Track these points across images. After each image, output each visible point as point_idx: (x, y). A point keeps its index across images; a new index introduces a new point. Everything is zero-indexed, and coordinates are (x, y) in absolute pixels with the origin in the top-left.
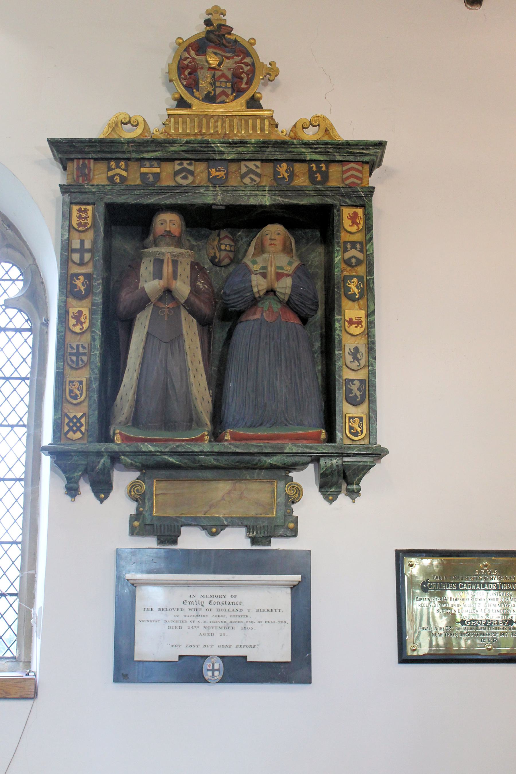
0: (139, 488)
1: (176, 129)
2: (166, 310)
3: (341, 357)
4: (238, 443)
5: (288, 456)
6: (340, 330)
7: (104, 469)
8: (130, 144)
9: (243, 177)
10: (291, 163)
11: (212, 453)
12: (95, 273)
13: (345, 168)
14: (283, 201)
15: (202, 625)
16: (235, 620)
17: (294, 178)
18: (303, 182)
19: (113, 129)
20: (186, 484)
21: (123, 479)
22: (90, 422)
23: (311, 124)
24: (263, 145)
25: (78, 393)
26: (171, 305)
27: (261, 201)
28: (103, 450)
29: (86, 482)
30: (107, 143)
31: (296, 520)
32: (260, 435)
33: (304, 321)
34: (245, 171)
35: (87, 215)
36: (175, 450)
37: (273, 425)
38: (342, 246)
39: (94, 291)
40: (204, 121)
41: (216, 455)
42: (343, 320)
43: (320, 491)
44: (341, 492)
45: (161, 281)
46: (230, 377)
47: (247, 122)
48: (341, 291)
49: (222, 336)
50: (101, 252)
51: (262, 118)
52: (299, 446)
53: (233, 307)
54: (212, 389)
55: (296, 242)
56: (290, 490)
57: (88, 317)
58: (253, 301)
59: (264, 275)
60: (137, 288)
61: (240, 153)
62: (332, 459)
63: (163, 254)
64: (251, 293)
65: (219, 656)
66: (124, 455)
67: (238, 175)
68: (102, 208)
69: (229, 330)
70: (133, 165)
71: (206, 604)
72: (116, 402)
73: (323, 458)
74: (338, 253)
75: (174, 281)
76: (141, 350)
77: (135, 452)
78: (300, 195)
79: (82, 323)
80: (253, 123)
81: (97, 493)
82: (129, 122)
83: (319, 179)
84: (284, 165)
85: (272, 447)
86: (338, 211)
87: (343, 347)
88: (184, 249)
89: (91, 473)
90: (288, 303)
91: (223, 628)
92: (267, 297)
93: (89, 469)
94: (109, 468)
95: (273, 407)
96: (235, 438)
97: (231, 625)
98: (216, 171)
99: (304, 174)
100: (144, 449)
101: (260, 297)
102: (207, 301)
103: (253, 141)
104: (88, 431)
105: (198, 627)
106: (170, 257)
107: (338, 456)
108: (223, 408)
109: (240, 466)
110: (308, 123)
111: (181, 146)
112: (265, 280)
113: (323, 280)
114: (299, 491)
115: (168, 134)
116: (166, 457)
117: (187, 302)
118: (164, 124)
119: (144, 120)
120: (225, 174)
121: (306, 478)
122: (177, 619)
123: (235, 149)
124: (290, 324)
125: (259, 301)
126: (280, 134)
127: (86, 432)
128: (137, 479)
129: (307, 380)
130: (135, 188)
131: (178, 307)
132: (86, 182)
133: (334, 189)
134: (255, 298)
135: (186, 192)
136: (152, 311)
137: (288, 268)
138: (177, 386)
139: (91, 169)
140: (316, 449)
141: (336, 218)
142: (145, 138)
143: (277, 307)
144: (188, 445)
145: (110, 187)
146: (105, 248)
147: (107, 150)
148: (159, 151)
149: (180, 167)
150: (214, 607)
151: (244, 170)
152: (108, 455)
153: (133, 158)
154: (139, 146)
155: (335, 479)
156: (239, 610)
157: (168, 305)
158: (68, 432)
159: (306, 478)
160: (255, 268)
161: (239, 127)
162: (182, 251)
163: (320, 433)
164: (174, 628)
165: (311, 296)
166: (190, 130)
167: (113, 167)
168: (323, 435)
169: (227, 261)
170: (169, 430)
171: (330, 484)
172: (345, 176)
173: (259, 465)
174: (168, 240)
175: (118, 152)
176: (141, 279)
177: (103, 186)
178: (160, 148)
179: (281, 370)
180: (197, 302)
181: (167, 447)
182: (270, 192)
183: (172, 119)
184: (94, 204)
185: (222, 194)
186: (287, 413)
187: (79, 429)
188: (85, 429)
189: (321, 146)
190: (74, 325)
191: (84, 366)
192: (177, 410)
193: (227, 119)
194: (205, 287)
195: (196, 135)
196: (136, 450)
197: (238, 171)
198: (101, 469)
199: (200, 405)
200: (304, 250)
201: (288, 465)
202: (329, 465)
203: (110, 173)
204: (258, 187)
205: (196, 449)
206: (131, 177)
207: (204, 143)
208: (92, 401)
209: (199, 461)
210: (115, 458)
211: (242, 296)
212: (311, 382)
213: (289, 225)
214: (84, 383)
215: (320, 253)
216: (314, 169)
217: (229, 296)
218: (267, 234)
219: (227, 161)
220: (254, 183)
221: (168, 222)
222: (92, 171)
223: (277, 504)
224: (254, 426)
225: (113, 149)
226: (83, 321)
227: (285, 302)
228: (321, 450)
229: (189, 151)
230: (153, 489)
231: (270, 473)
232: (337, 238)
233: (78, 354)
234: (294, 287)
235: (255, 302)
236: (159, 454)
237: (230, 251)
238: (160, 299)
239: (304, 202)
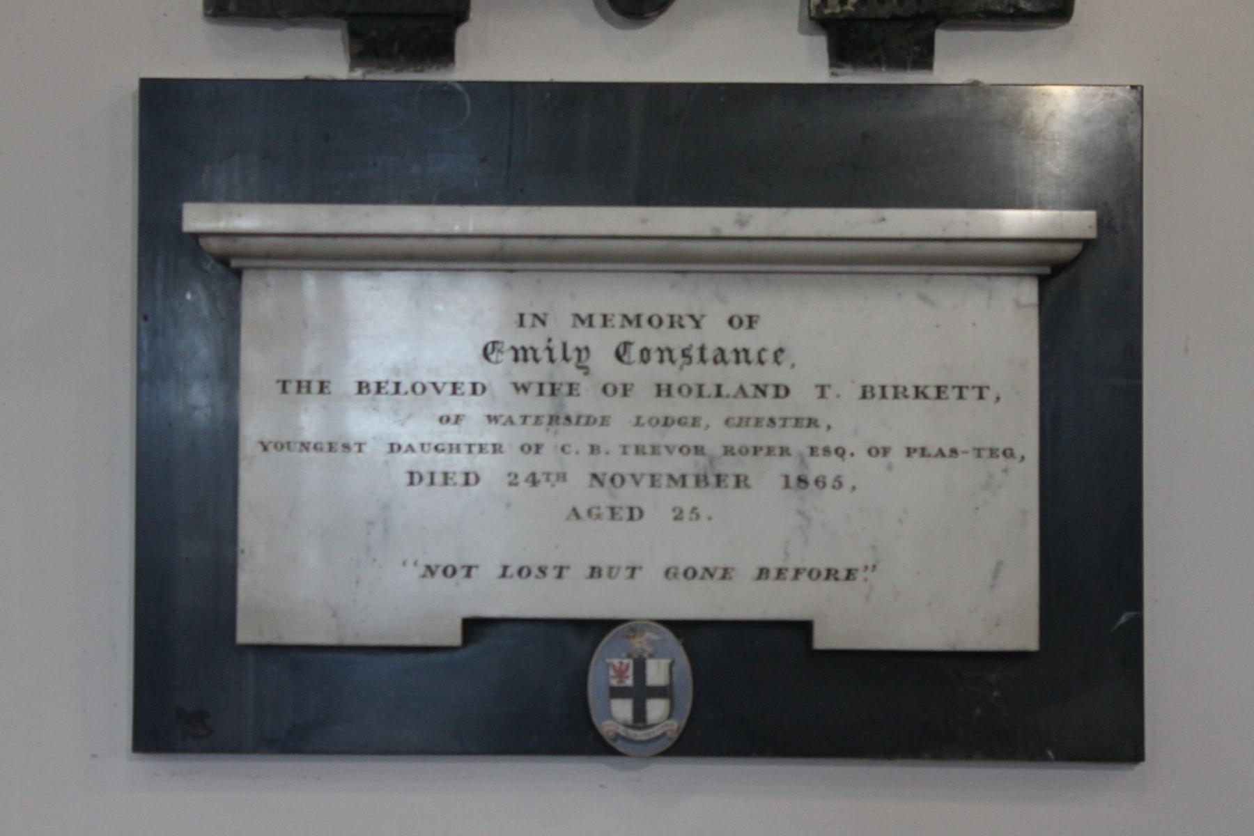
15: (579, 467)
16: (750, 443)
65: (672, 625)
71: (604, 366)
91: (691, 481)
97: (729, 466)
105: (562, 477)
122: (451, 434)
150: (644, 375)
156: (771, 391)
164: (439, 479)
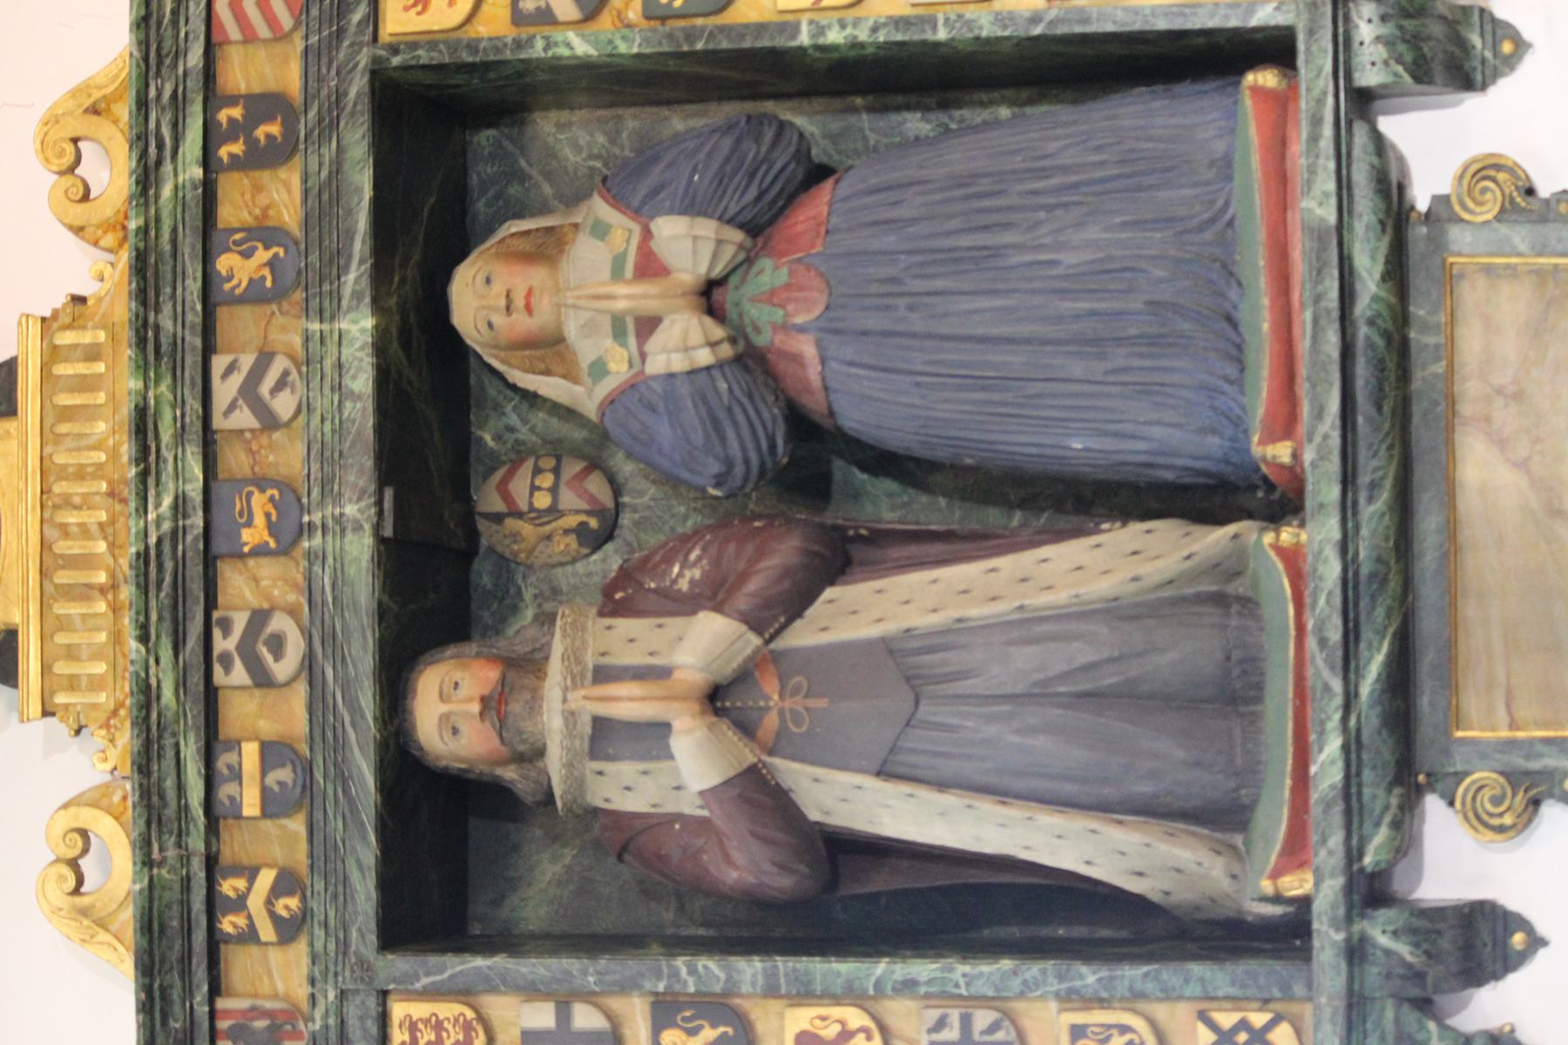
0: (1486, 794)
1: (96, 684)
2: (787, 704)
3: (960, 16)
4: (1305, 410)
5: (1350, 212)
6: (855, 25)
7: (1414, 931)
8: (156, 855)
9: (269, 421)
10: (216, 239)
11: (1348, 509)
12: (648, 985)
13: (234, 33)
14: (361, 262)
17: (271, 223)
18: (289, 192)
19: (102, 924)
20: (1469, 610)
21: (1454, 860)
22: (1232, 991)
23: (71, 170)
24: (147, 341)
26: (770, 686)
27: (362, 348)
28: (1340, 937)
29: (1464, 1005)
30: (151, 942)
32: (1274, 324)
33: (819, 173)
34: (245, 408)
35: (426, 1022)
36: (1339, 654)
37: (1232, 274)
38: (532, 30)
39: (717, 988)
40: (63, 577)
41: (1355, 493)
42: (816, 16)
43: (1484, 87)
44: (1482, 11)
45: (677, 725)
46: (1048, 452)
47: (66, 414)
48: (703, 29)
49: (890, 495)
50: (570, 964)
51: (53, 354)
52: (1312, 170)
53: (772, 447)
54: (1098, 524)
55: (519, 215)
56: (1481, 204)
57: (823, 1011)
58: (747, 369)
59: (648, 325)
60: (704, 823)
61: (181, 435)
62: (1356, 39)
63: (570, 717)
64: (716, 373)
66: (1361, 855)
67: (264, 440)
68: (399, 963)
69: (864, 469)
70: (234, 845)
72: (1155, 897)
73: (1356, 75)
74: (556, 44)
75: (677, 675)
76: (949, 800)
77: (1348, 812)
78: (337, 198)
80: (72, 390)
81: (1508, 962)
82: (73, 864)
83: (274, 129)
84: (224, 263)
85: (1319, 272)
86: (394, 49)
87: (921, 11)
88: (549, 644)
89: (1430, 980)
90: (754, 229)
92: (732, 313)
93: (1415, 992)
94: (1412, 914)
95: (1159, 273)
96: (1285, 423)
98: (249, 524)
99: (258, 189)
100: (1336, 775)
101: (733, 340)
102: (750, 548)
103: (135, 384)
104: (1266, 1001)
106: (583, 692)
107: (1347, 18)
108: (1169, 476)
109: (1395, 396)
110: (68, 180)
111: (157, 662)
112: (666, 323)
113: (665, 112)
114: (1486, 170)
115: (115, 713)
116: (1367, 687)
117: (755, 623)
118: (78, 732)
119: (65, 806)
120: (262, 491)
121: (1433, 143)
123: (164, 452)
124: (834, 220)
125: (749, 343)
126: (107, 285)
127: (1272, 1006)
128: (1451, 804)
129: (1052, 147)
130: (318, 838)
131: (776, 657)
132: (301, 1025)
133: (313, 70)
134: (738, 359)
135: (329, 638)
136: (794, 758)
137: (618, 238)
138: (1083, 654)
139: (253, 1009)
140: (1320, 101)
141: (424, 56)
142: (130, 803)
143: (770, 274)
144: (1315, 603)
145: (319, 933)
146: (555, 952)
147: (177, 947)
148: (177, 745)
149: (238, 665)
151: (244, 418)
152: (1363, 916)
153: (208, 844)
154: (160, 820)
155: (1436, 29)
157: (767, 698)
159: (1433, 143)
160: (619, 368)
161: (82, 443)
162: (558, 648)
163: (1257, 91)
165: (727, 143)
166: (98, 629)
167: (241, 921)
168: (1266, 78)
169: (597, 485)
170: (1260, 687)
171: (1454, 49)
172: (263, 31)
173: (1389, 325)
174: (516, 707)
175: (186, 905)
176: (669, 808)
177: (314, 959)
178: (168, 741)
179: (1017, 247)
180: (753, 585)
181: (1327, 688)
182: (327, 314)
183: (61, 699)
184: (384, 994)
185: (338, 499)
186: (1182, 219)
188: (1260, 1010)
189: (152, 125)
191: (1014, 1023)
192: (1185, 653)
193: (57, 489)
194: (699, 559)
195: (115, 609)
196: (1339, 808)
197: (249, 442)
198: (1417, 945)
199: (1160, 564)
200: (547, 189)
201: (1388, 210)
202: (1381, 52)
203: (267, 932)
204: (308, 362)
205: (1331, 570)
206: (278, 853)
207: (146, 574)
208: (1150, 987)
209: (1379, 560)
210: (1370, 891)
211: (729, 410)
212: (1059, 131)
213: (454, 243)
214: (1080, 1018)
215: (561, 127)
216: (237, 148)
217: (729, 464)
218: (490, 325)
219: (214, 486)
220: (294, 375)
221: (449, 709)
222: (259, 1002)
223: (1540, 254)
224: (1239, 347)
225: (175, 923)
226: (836, 1028)
227: (748, 243)
228: (1325, 82)
229: (176, 631)
230: (1487, 743)
231: (1418, 281)
232: (497, 50)
234: (691, 207)
235: (751, 361)
236: (1353, 722)
237: (556, 471)
238: (746, 729)
239: (362, 181)
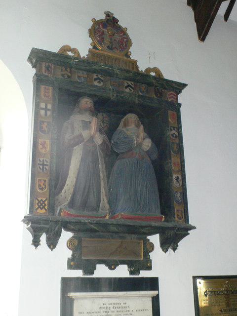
21: (66, 236)
25: (43, 186)
31: (150, 261)
66: (70, 224)
71: (111, 309)
79: (45, 148)
81: (49, 246)
83: (159, 95)
114: (152, 247)
116: (92, 226)
150: (116, 310)
158: (37, 209)
159: (155, 239)
168: (163, 219)
187: (44, 207)
190: (41, 149)
203: (63, 73)
233: (43, 165)
238: (88, 141)
